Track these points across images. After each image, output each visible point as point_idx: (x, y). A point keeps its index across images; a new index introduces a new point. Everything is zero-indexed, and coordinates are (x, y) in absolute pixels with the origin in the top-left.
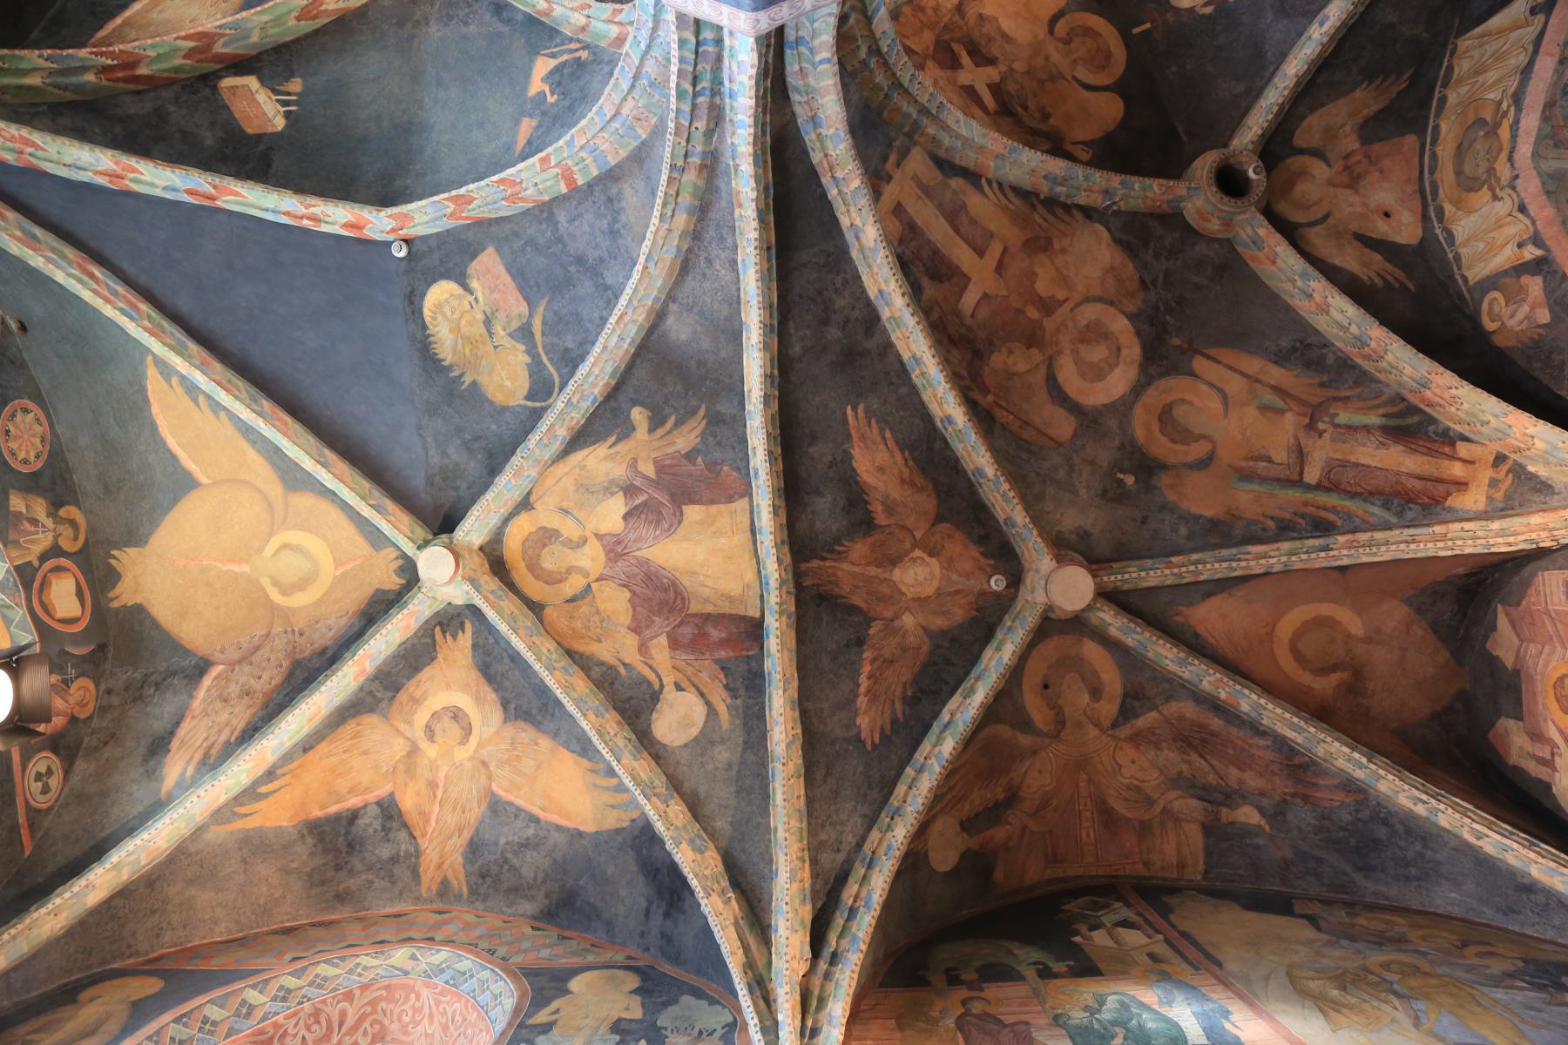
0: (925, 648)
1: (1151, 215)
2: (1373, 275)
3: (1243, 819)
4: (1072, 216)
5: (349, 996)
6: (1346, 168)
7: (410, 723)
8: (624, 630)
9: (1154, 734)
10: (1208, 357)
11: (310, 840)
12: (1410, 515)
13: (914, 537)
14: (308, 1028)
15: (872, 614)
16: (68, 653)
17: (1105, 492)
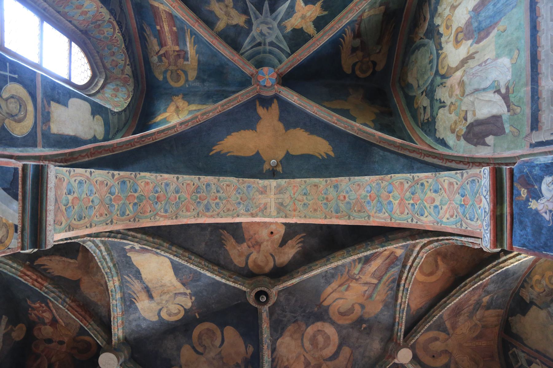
1: (270, 319)
2: (297, 246)
3: (487, 300)
4: (275, 358)
6: (253, 247)
9: (453, 323)
10: (323, 301)
12: (398, 263)
17: (368, 334)
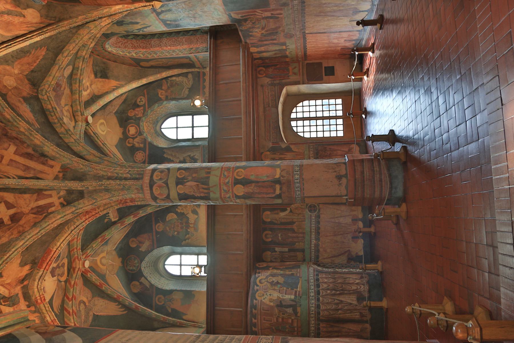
0: (16, 63)
5: (119, 47)
7: (90, 91)
8: (65, 95)
11: (108, 76)
13: (11, 92)
14: (128, 46)
15: (25, 77)
16: (134, 120)
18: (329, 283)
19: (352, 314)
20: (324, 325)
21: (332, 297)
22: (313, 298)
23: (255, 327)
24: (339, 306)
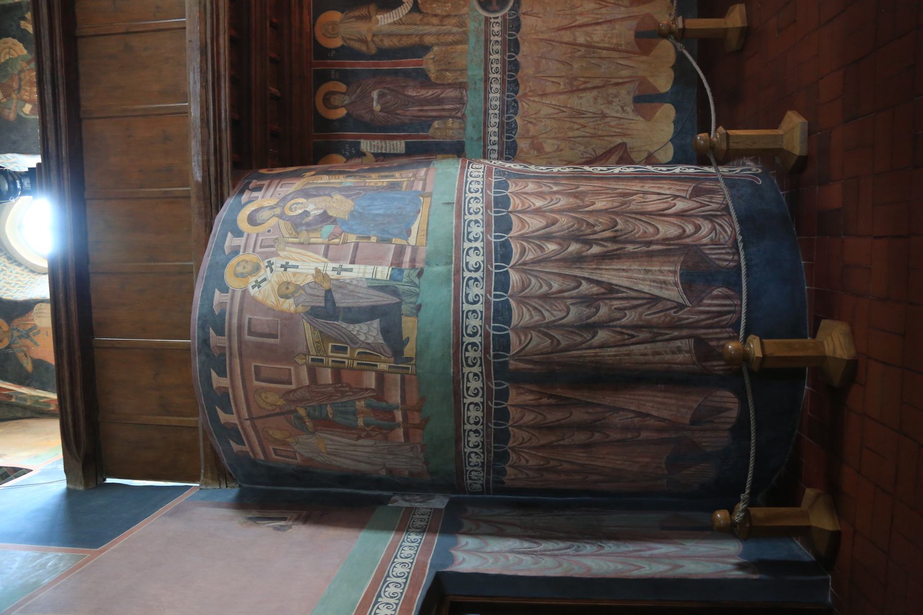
18: (552, 211)
19: (659, 346)
20: (528, 398)
21: (567, 272)
22: (478, 275)
23: (227, 410)
24: (598, 309)
